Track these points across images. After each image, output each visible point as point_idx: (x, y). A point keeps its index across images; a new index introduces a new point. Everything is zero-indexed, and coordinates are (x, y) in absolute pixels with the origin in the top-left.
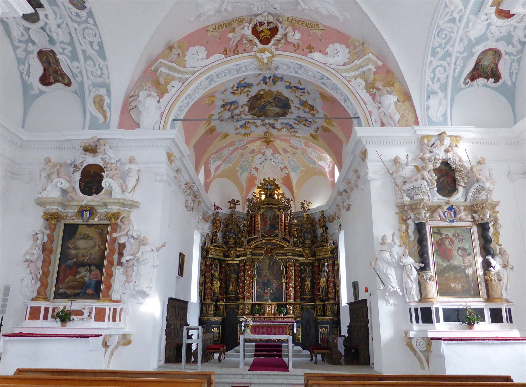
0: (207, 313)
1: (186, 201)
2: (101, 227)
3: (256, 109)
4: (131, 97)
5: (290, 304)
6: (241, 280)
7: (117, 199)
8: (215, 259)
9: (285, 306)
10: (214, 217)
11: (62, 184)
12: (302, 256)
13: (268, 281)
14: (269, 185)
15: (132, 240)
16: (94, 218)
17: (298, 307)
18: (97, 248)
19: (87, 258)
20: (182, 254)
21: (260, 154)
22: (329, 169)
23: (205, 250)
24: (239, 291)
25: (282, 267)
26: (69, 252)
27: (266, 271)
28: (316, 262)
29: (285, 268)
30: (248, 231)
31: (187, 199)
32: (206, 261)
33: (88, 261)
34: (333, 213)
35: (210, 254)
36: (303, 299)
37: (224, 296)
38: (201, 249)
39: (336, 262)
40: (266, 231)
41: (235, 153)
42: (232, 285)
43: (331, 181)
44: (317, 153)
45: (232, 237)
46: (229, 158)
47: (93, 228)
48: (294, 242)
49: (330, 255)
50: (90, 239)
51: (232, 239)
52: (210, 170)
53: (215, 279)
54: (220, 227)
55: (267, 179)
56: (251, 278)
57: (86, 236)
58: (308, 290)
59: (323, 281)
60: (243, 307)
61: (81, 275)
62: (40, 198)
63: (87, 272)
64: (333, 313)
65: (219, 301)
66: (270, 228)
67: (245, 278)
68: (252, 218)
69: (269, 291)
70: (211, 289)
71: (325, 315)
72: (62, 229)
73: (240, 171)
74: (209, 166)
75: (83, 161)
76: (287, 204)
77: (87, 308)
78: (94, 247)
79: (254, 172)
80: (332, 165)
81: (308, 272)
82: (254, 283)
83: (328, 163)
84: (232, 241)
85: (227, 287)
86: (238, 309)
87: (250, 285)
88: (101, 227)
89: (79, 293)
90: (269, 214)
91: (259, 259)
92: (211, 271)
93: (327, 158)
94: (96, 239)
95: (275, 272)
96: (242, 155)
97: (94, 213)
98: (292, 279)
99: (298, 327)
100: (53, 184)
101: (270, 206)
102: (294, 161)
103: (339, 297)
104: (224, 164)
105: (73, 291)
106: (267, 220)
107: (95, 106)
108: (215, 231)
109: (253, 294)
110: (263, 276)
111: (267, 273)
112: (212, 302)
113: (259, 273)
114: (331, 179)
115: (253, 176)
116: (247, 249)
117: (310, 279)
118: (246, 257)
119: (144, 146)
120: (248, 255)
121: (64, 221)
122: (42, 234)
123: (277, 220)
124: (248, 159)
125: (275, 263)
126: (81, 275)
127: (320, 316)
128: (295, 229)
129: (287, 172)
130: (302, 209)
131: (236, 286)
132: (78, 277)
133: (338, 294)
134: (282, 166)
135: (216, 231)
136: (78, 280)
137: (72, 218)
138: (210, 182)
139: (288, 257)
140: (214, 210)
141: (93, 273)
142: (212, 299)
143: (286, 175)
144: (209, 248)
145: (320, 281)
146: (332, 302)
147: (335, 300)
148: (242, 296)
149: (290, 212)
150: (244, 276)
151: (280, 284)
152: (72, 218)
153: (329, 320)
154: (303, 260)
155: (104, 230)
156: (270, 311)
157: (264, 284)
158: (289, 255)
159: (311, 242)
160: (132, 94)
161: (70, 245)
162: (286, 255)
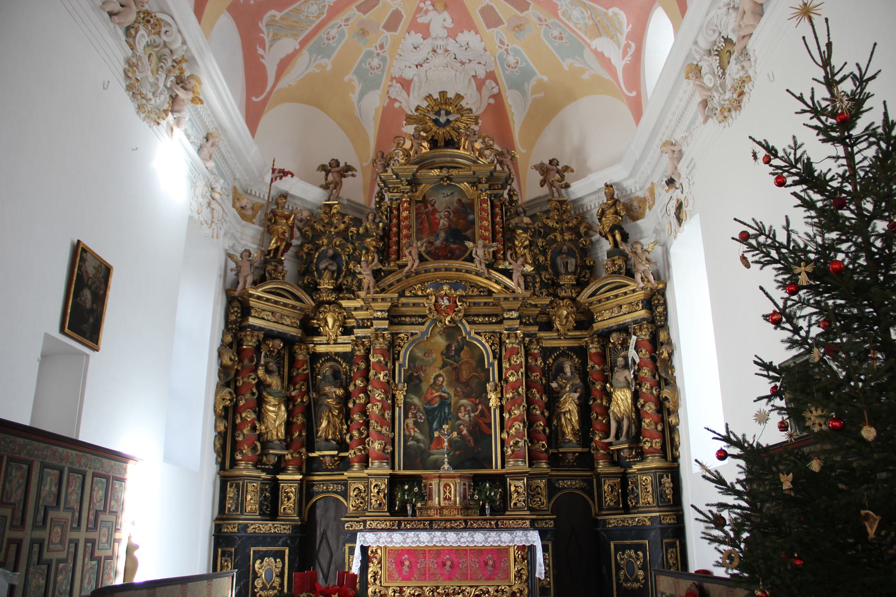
0: (241, 505)
1: (130, 66)
5: (517, 476)
6: (354, 402)
8: (270, 335)
9: (500, 480)
10: (274, 207)
12: (548, 326)
13: (444, 402)
14: (443, 112)
17: (542, 485)
20: (85, 250)
21: (416, 33)
22: (623, 63)
23: (236, 304)
24: (348, 437)
25: (489, 359)
27: (434, 372)
28: (592, 343)
29: (496, 363)
30: (379, 251)
31: (134, 60)
32: (241, 340)
34: (641, 190)
35: (255, 317)
36: (555, 461)
37: (300, 453)
38: (222, 301)
39: (662, 336)
40: (437, 248)
41: (339, 20)
42: (328, 416)
43: (628, 98)
44: (589, 8)
45: (330, 270)
46: (322, 34)
48: (525, 275)
49: (642, 313)
51: (327, 275)
52: (263, 67)
53: (271, 399)
54: (292, 237)
55: (436, 96)
56: (386, 393)
58: (573, 429)
59: (622, 399)
60: (362, 487)
64: (660, 496)
65: (283, 470)
66: (446, 240)
67: (368, 396)
68: (391, 212)
69: (446, 434)
70: (254, 428)
71: (626, 510)
73: (358, 88)
74: (260, 51)
76: (499, 168)
79: (397, 91)
80: (633, 46)
81: (569, 374)
82: (397, 409)
83: (623, 41)
84: (326, 284)
85: (310, 426)
86: (345, 494)
87: (383, 415)
90: (442, 201)
91: (412, 334)
92: (255, 370)
93: (620, 23)
95: (465, 375)
96: (363, 33)
98: (519, 394)
99: (545, 549)
101: (445, 172)
102: (517, 53)
103: (675, 446)
104: (305, 52)
106: (437, 215)
108: (273, 246)
109: (393, 446)
110: (425, 387)
111: (441, 379)
112: (255, 473)
113: (413, 381)
114: (631, 92)
115: (397, 105)
116: (374, 300)
117: (576, 395)
118: (372, 330)
120: (378, 319)
123: (471, 217)
124: (382, 47)
125: (465, 347)
127: (614, 510)
128: (527, 243)
129: (496, 91)
130: (545, 190)
131: (342, 423)
133: (672, 440)
134: (482, 74)
135: (277, 249)
138: (263, 105)
139: (507, 324)
140: (272, 182)
142: (258, 463)
143: (492, 101)
144: (251, 295)
145: (610, 400)
146: (653, 462)
147: (664, 457)
148: (358, 453)
149: (509, 194)
150: (364, 390)
151: (482, 411)
153: (648, 523)
154: (550, 340)
156: (450, 499)
157: (429, 413)
158: (509, 319)
159: (577, 280)
162: (500, 322)
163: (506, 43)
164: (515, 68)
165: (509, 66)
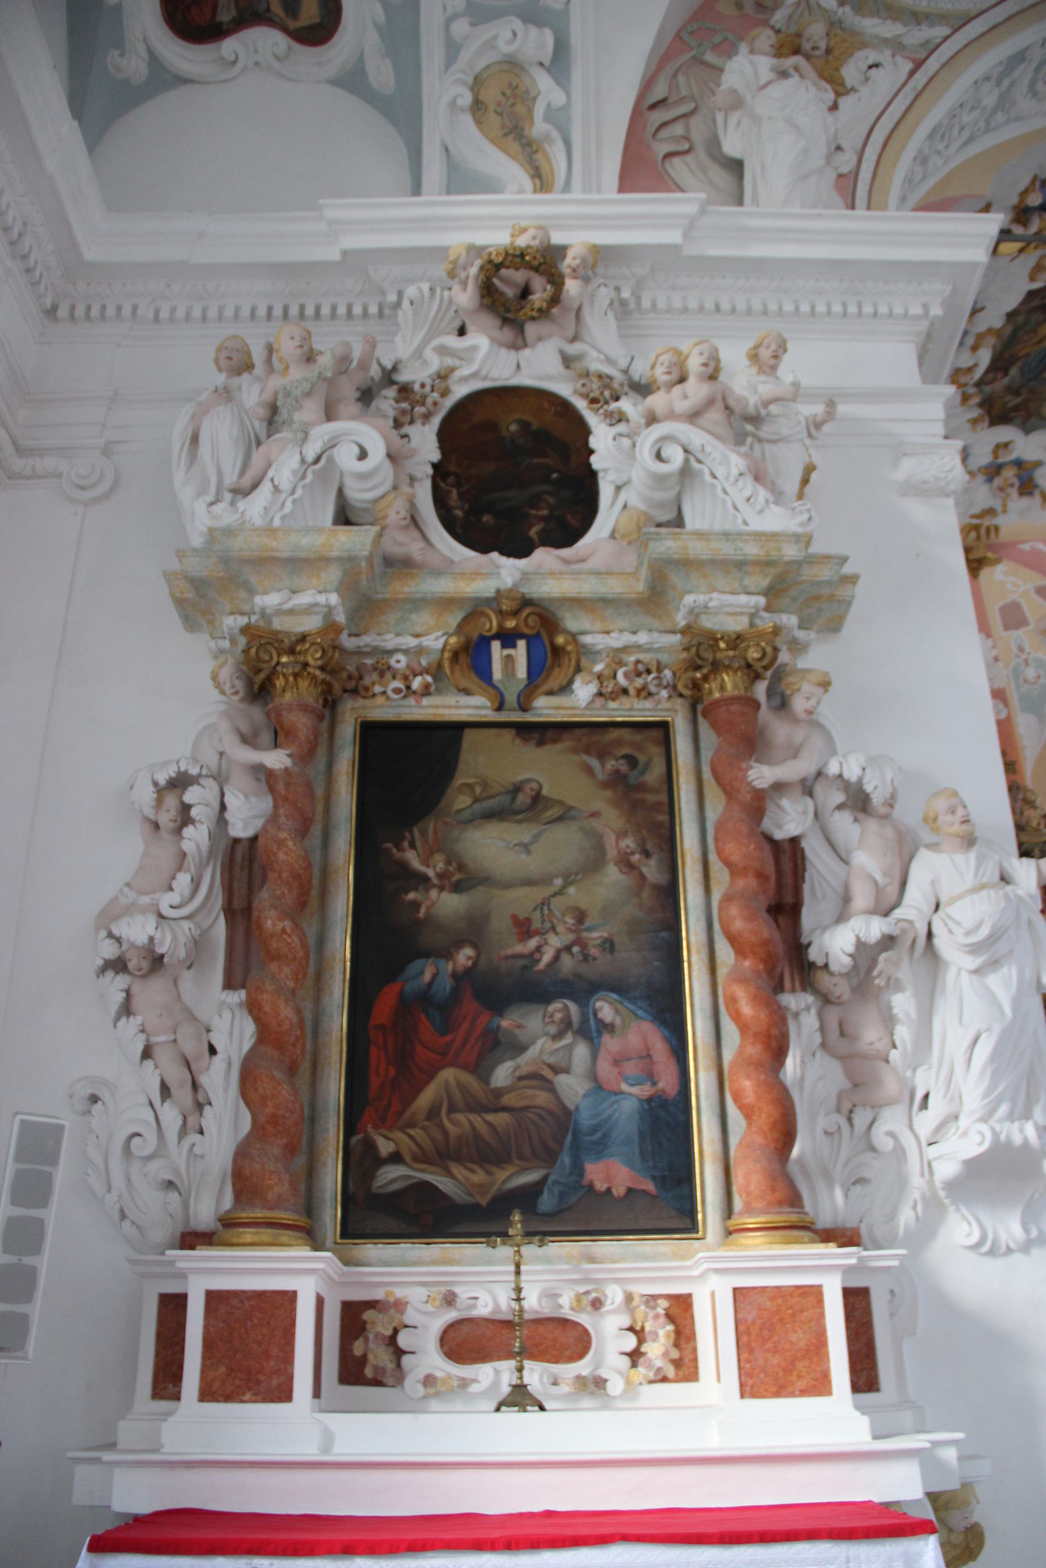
2: (619, 743)
3: (1014, 371)
4: (653, 106)
7: (760, 537)
11: (363, 455)
15: (843, 824)
16: (566, 688)
18: (613, 874)
19: (555, 942)
26: (416, 905)
33: (567, 963)
47: (559, 747)
50: (560, 819)
57: (523, 799)
61: (526, 1061)
62: (229, 532)
63: (568, 1039)
72: (346, 758)
75: (452, 370)
77: (614, 1295)
78: (595, 863)
88: (619, 743)
89: (535, 1190)
94: (595, 815)
97: (557, 652)
100: (311, 451)
105: (479, 1177)
107: (478, 122)
119: (797, 309)
121: (360, 702)
122: (211, 786)
126: (526, 1061)
132: (502, 1074)
136: (507, 1100)
137: (417, 683)
141: (610, 1043)
152: (417, 683)
155: (642, 759)
160: (659, 92)
161: (413, 860)
163: (1027, 649)
164: (1034, 683)
165: (1026, 681)
